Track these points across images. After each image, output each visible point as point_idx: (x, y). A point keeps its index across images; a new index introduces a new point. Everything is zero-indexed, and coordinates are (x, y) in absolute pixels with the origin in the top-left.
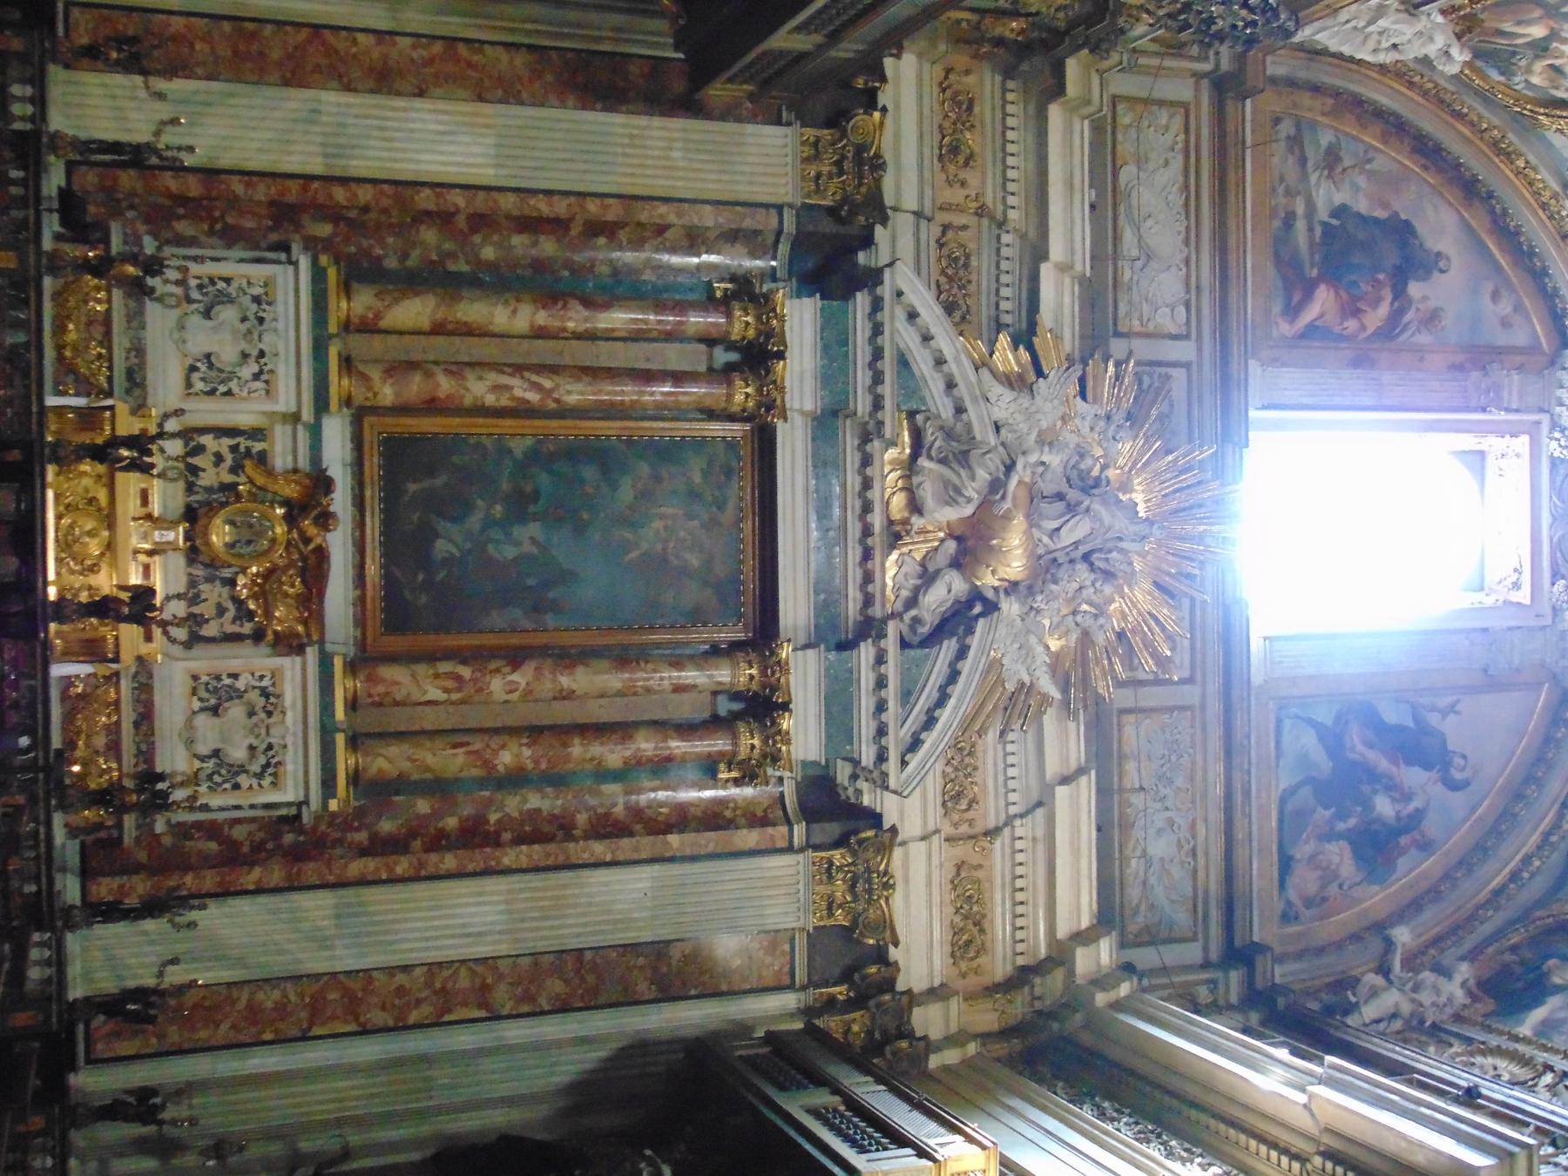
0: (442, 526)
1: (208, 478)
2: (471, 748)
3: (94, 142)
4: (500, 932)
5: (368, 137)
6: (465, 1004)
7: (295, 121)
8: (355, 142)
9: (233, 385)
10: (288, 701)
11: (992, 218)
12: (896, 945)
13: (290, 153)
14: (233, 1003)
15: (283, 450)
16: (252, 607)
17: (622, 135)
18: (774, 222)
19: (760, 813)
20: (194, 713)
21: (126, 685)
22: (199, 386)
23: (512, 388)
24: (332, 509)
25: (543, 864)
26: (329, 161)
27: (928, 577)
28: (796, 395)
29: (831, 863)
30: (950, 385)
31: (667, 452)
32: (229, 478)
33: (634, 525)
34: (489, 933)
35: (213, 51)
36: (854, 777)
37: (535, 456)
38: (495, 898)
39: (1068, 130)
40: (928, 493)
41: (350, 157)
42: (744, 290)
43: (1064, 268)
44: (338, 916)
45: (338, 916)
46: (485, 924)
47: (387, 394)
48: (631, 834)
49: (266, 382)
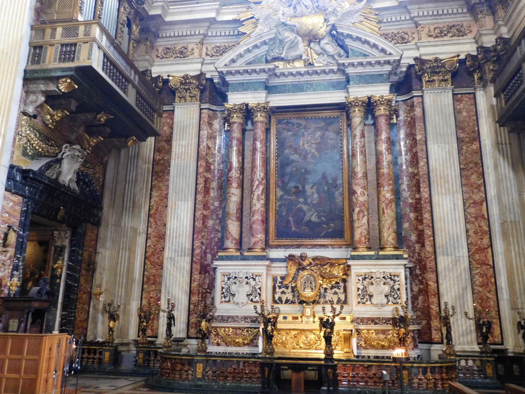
0: (306, 219)
1: (290, 296)
2: (385, 207)
3: (167, 333)
4: (453, 197)
5: (179, 242)
6: (481, 210)
7: (174, 265)
8: (180, 247)
9: (257, 287)
10: (368, 271)
11: (203, 39)
12: (459, 56)
13: (184, 267)
14: (480, 292)
15: (280, 270)
16: (334, 283)
17: (178, 161)
18: (205, 111)
19: (409, 108)
21: (361, 327)
22: (257, 298)
23: (258, 195)
24: (299, 255)
25: (428, 183)
26: (186, 255)
27: (324, 52)
28: (260, 99)
29: (428, 81)
30: (256, 47)
31: (281, 144)
32: (290, 290)
33: (306, 154)
34: (454, 201)
35: (153, 291)
36: (395, 74)
38: (440, 199)
39: (173, 14)
40: (293, 54)
41: (185, 248)
42: (226, 120)
43: (218, 12)
44: (447, 255)
45: (447, 255)
46: (450, 204)
47: (261, 236)
48: (417, 152)
49: (256, 276)
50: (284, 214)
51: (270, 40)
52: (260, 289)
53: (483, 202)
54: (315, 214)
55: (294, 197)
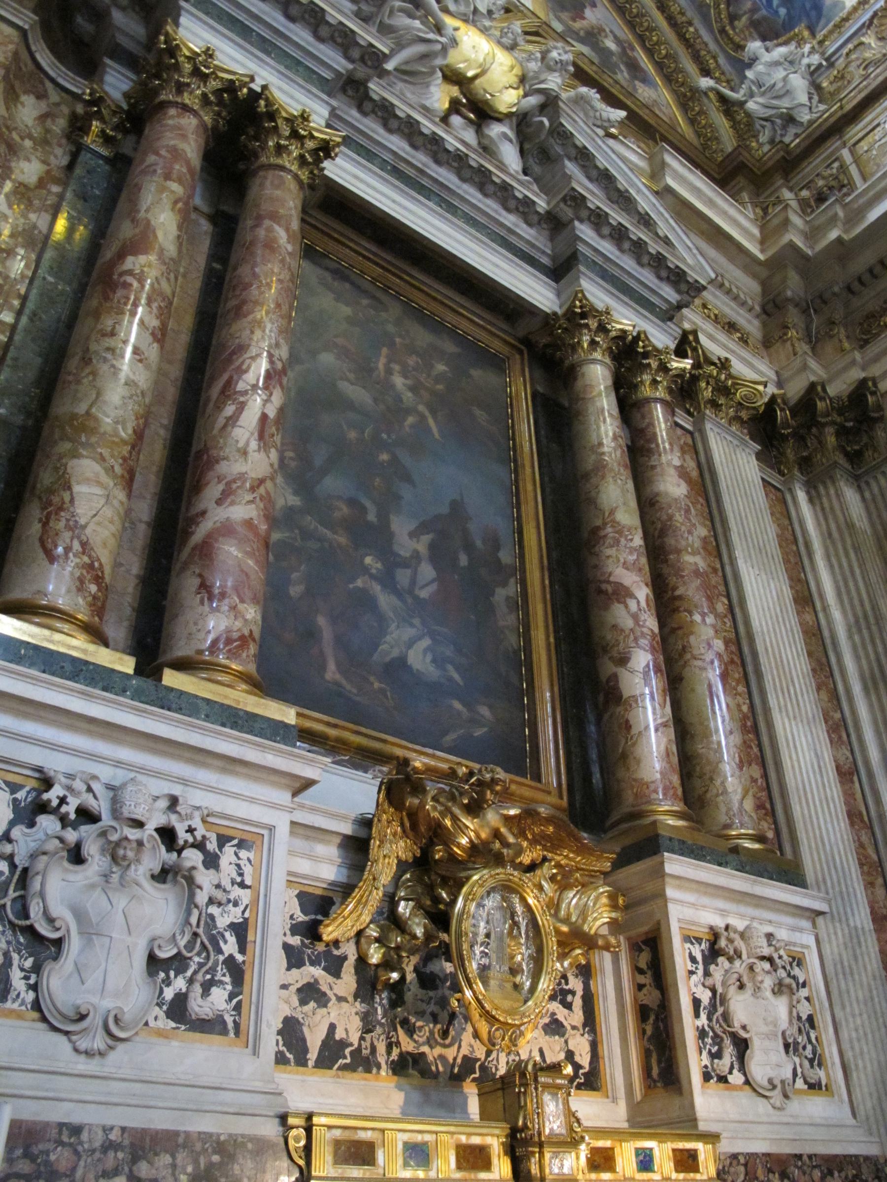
20: (747, 1082)
22: (219, 998)
49: (223, 840)
50: (295, 591)
52: (240, 930)
53: (852, 774)
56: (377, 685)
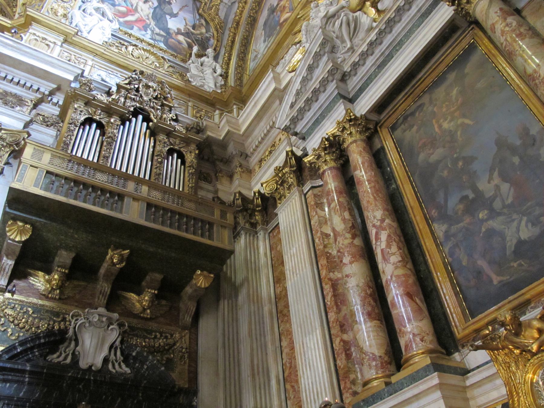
23: (382, 250)
33: (452, 134)
37: (444, 217)
39: (244, 122)
50: (464, 263)
51: (323, 45)
54: (523, 223)
55: (467, 219)
56: (515, 265)
